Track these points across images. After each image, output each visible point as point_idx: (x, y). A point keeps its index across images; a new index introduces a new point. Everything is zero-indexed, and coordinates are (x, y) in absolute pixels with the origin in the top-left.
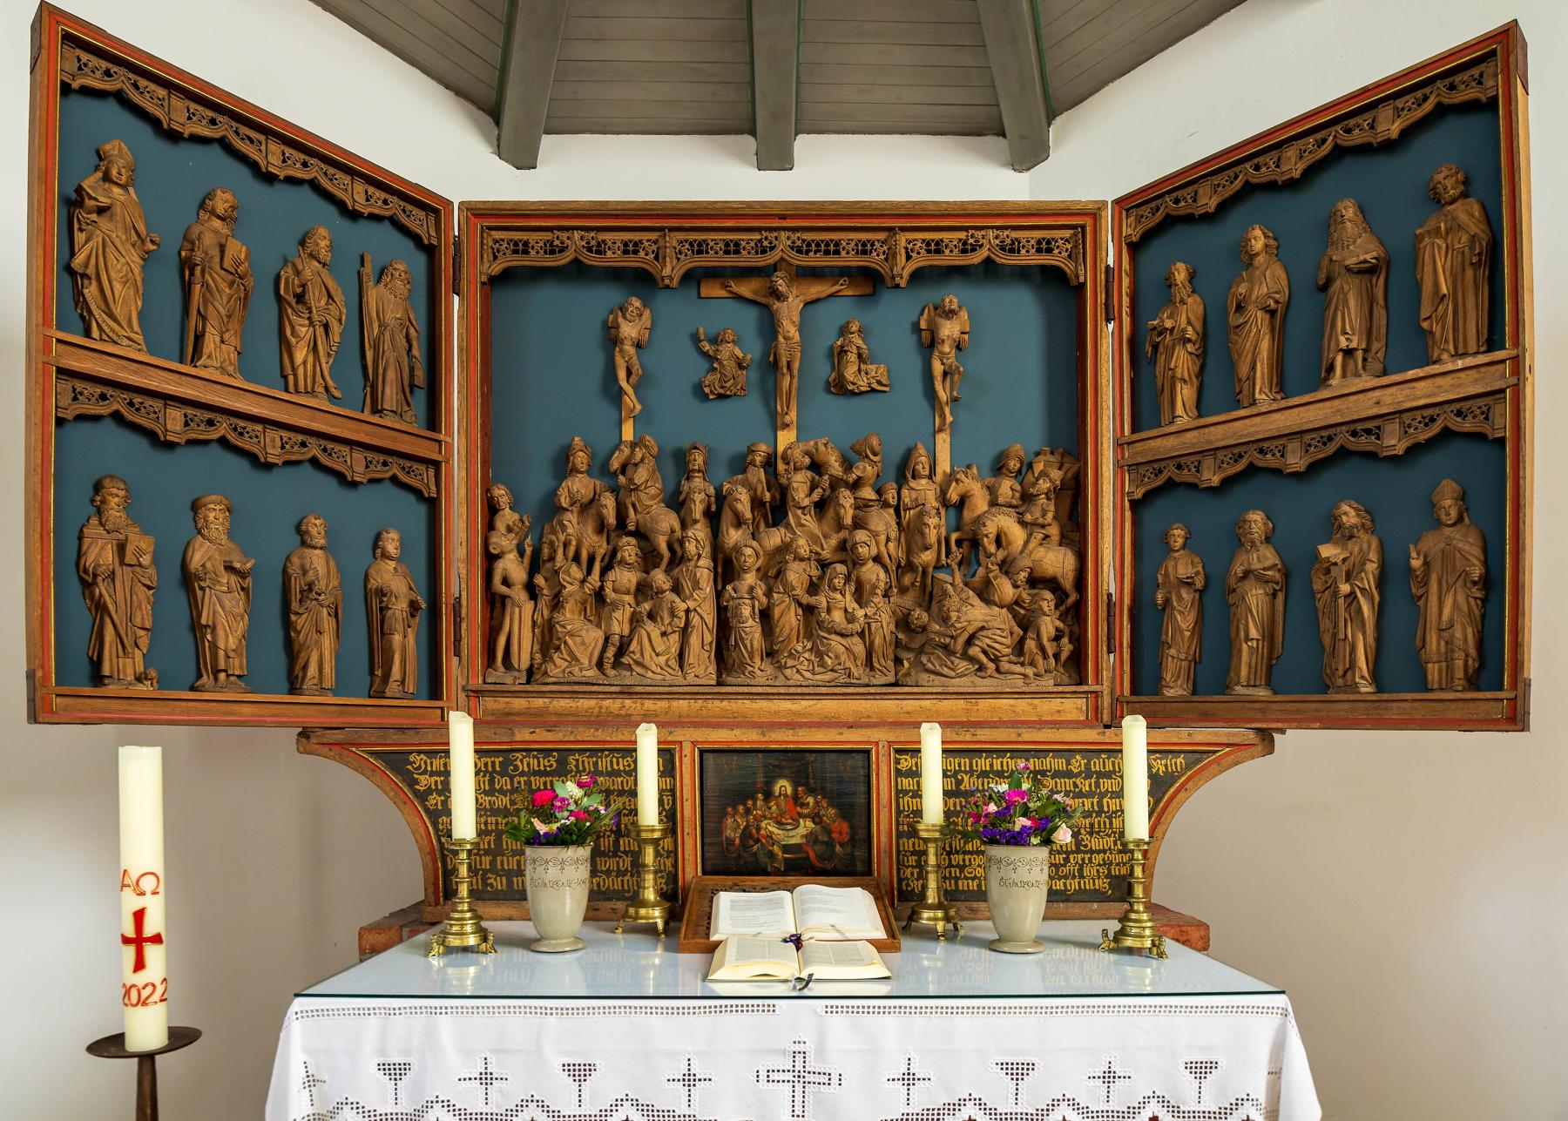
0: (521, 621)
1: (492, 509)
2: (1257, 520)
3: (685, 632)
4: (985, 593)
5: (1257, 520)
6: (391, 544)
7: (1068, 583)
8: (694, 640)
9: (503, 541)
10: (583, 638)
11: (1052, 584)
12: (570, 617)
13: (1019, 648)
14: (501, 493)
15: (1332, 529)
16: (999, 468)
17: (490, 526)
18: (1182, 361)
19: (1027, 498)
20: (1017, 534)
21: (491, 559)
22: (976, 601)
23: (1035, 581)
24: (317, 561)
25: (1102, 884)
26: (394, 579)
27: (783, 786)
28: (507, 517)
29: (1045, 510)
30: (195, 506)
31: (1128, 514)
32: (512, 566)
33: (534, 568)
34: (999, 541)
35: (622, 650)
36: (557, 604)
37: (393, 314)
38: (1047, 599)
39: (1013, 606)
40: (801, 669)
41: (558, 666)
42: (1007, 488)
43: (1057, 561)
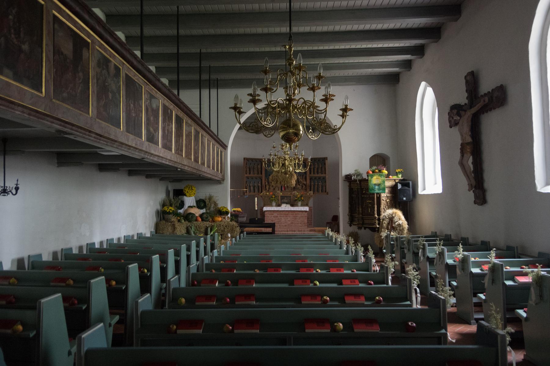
0: (267, 187)
1: (265, 179)
2: (316, 181)
3: (279, 188)
4: (299, 185)
5: (316, 181)
6: (260, 182)
7: (306, 184)
8: (279, 188)
9: (266, 181)
10: (272, 188)
11: (305, 184)
12: (271, 187)
13: (302, 189)
14: (266, 178)
15: (319, 182)
16: (301, 176)
17: (265, 181)
18: (312, 170)
19: (303, 178)
20: (302, 180)
21: (265, 183)
22: (299, 186)
23: (303, 184)
24: (255, 184)
25: (306, 204)
26: (260, 185)
27: (286, 198)
28: (266, 180)
29: (304, 179)
30: (250, 182)
31: (309, 180)
32: (267, 183)
33: (268, 183)
34: (301, 181)
35: (274, 189)
36: (270, 186)
37: (259, 167)
38: (304, 185)
39: (302, 186)
40: (287, 190)
41: (270, 190)
42: (301, 177)
43: (305, 183)
